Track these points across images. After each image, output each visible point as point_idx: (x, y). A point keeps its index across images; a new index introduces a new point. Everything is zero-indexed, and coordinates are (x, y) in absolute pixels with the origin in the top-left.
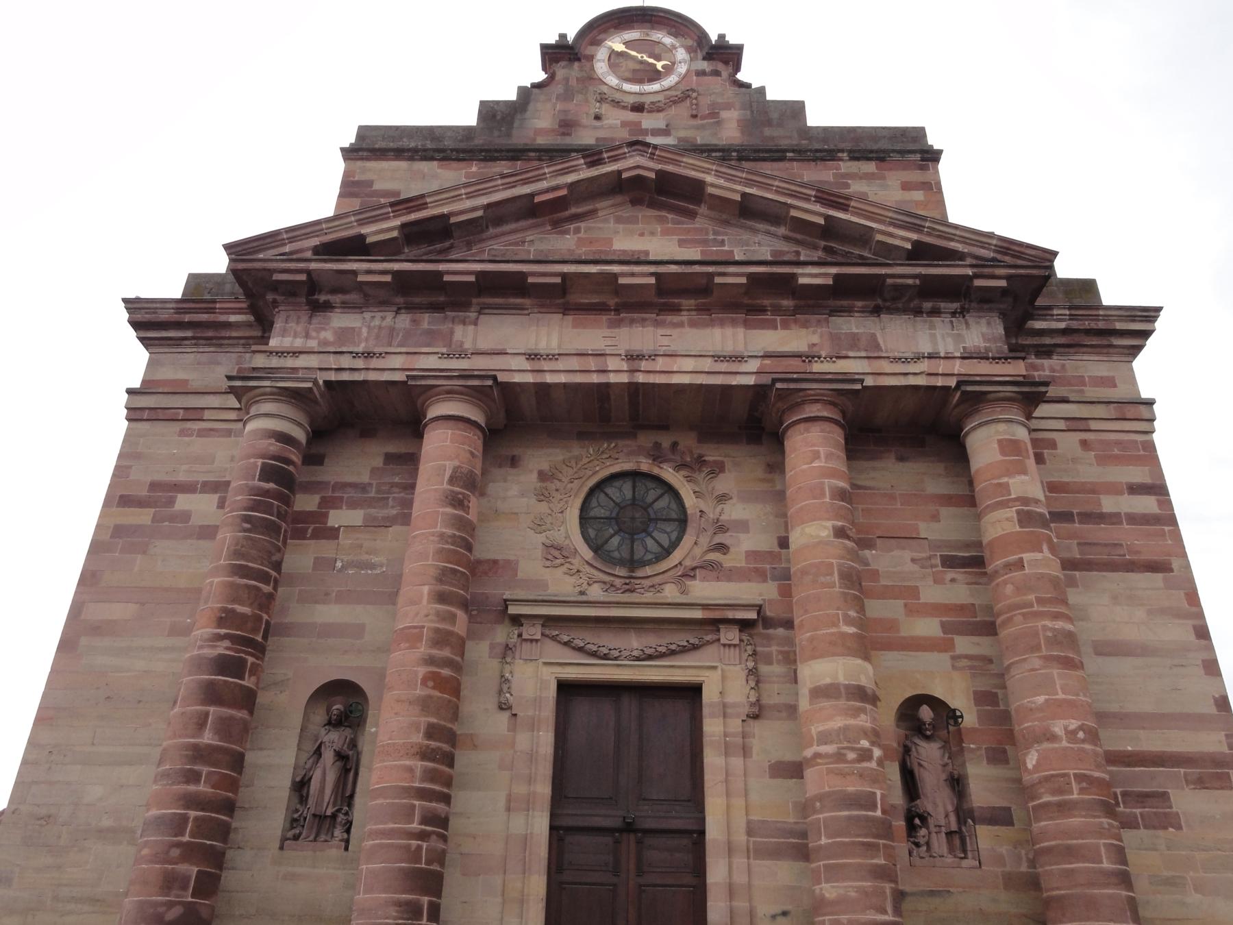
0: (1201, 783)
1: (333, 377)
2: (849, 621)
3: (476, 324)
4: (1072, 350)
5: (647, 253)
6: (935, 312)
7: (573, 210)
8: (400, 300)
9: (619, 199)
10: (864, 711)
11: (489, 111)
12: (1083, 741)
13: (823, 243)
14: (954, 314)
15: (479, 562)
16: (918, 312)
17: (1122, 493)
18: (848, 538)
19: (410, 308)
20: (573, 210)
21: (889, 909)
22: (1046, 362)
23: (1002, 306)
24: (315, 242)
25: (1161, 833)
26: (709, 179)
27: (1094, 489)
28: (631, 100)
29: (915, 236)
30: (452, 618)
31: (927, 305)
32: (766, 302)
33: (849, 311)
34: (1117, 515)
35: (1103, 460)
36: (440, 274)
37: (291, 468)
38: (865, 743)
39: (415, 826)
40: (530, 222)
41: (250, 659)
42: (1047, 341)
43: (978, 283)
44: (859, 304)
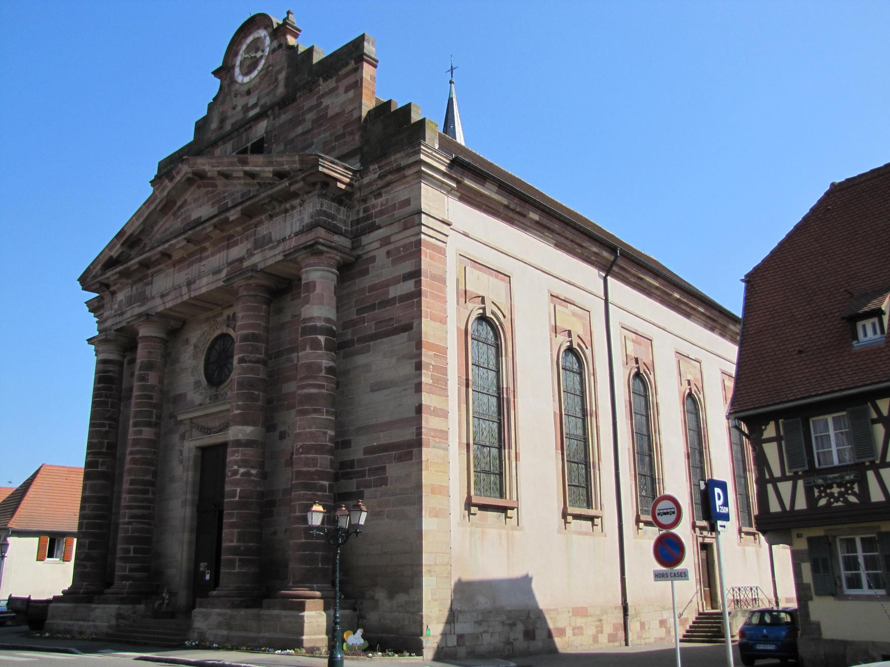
0: (400, 459)
1: (115, 328)
2: (238, 408)
3: (151, 283)
4: (389, 188)
5: (200, 217)
6: (293, 208)
7: (178, 204)
8: (130, 281)
9: (192, 188)
10: (238, 452)
11: (201, 126)
12: (302, 453)
13: (255, 181)
14: (301, 205)
15: (181, 395)
16: (286, 211)
17: (399, 283)
18: (245, 362)
19: (135, 283)
20: (178, 204)
21: (235, 541)
22: (379, 201)
23: (317, 192)
24: (99, 267)
25: (379, 489)
26: (207, 168)
27: (387, 285)
28: (245, 88)
29: (271, 169)
30: (140, 432)
31: (288, 206)
32: (231, 232)
33: (261, 223)
34: (395, 298)
35: (395, 262)
36: (128, 268)
37: (110, 374)
38: (236, 467)
39: (127, 520)
40: (164, 220)
41: (100, 460)
42: (374, 187)
43: (293, 188)
44: (263, 217)
